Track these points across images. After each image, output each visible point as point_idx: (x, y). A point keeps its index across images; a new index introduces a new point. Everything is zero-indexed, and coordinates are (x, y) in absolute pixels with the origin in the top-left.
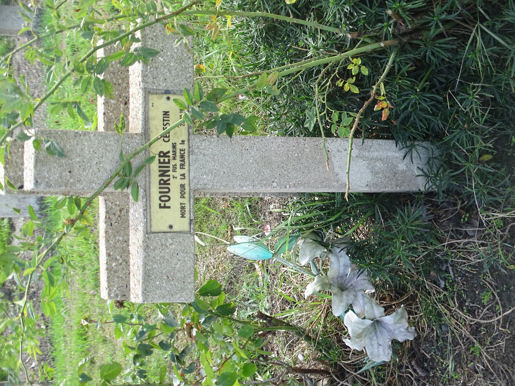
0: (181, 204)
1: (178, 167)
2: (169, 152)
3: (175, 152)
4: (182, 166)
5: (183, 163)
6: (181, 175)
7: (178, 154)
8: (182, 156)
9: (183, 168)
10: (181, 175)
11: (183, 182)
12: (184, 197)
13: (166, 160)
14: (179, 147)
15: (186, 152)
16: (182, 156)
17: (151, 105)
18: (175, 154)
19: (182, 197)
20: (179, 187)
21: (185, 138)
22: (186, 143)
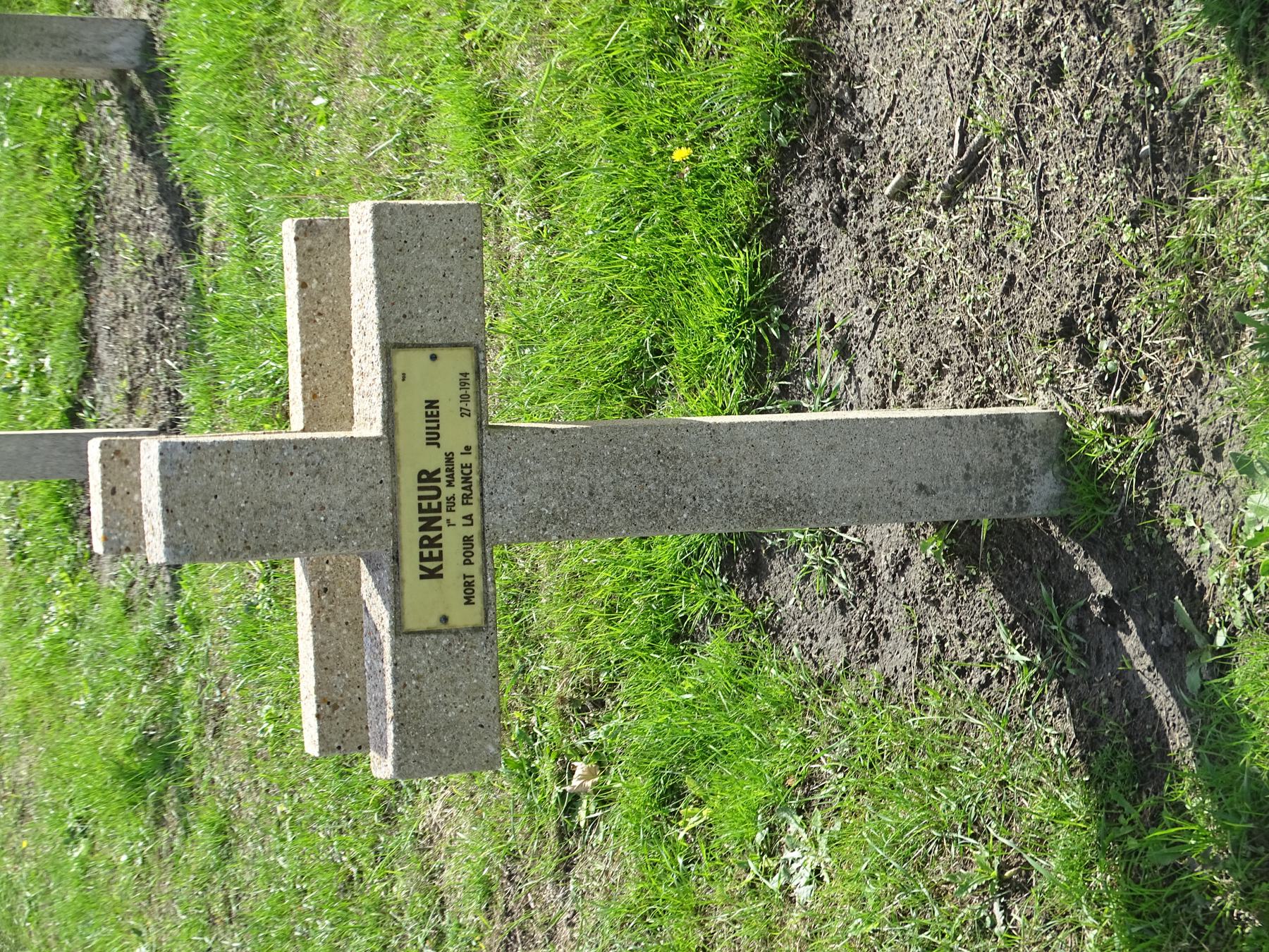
0: (465, 577)
1: (458, 500)
3: (452, 470)
4: (466, 499)
6: (464, 518)
7: (458, 477)
8: (466, 479)
9: (467, 503)
10: (464, 518)
12: (471, 563)
13: (434, 504)
14: (459, 460)
15: (474, 469)
18: (452, 476)
19: (468, 562)
21: (473, 443)
22: (474, 451)
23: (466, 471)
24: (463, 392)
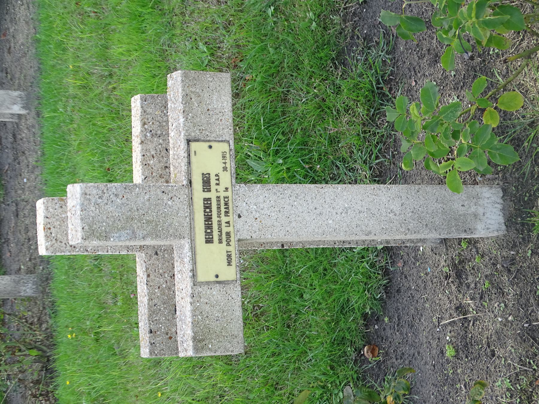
0: (227, 252)
4: (227, 213)
6: (226, 223)
8: (226, 204)
10: (226, 223)
12: (230, 245)
15: (230, 198)
17: (192, 154)
19: (228, 244)
21: (229, 186)
23: (226, 200)
24: (224, 161)
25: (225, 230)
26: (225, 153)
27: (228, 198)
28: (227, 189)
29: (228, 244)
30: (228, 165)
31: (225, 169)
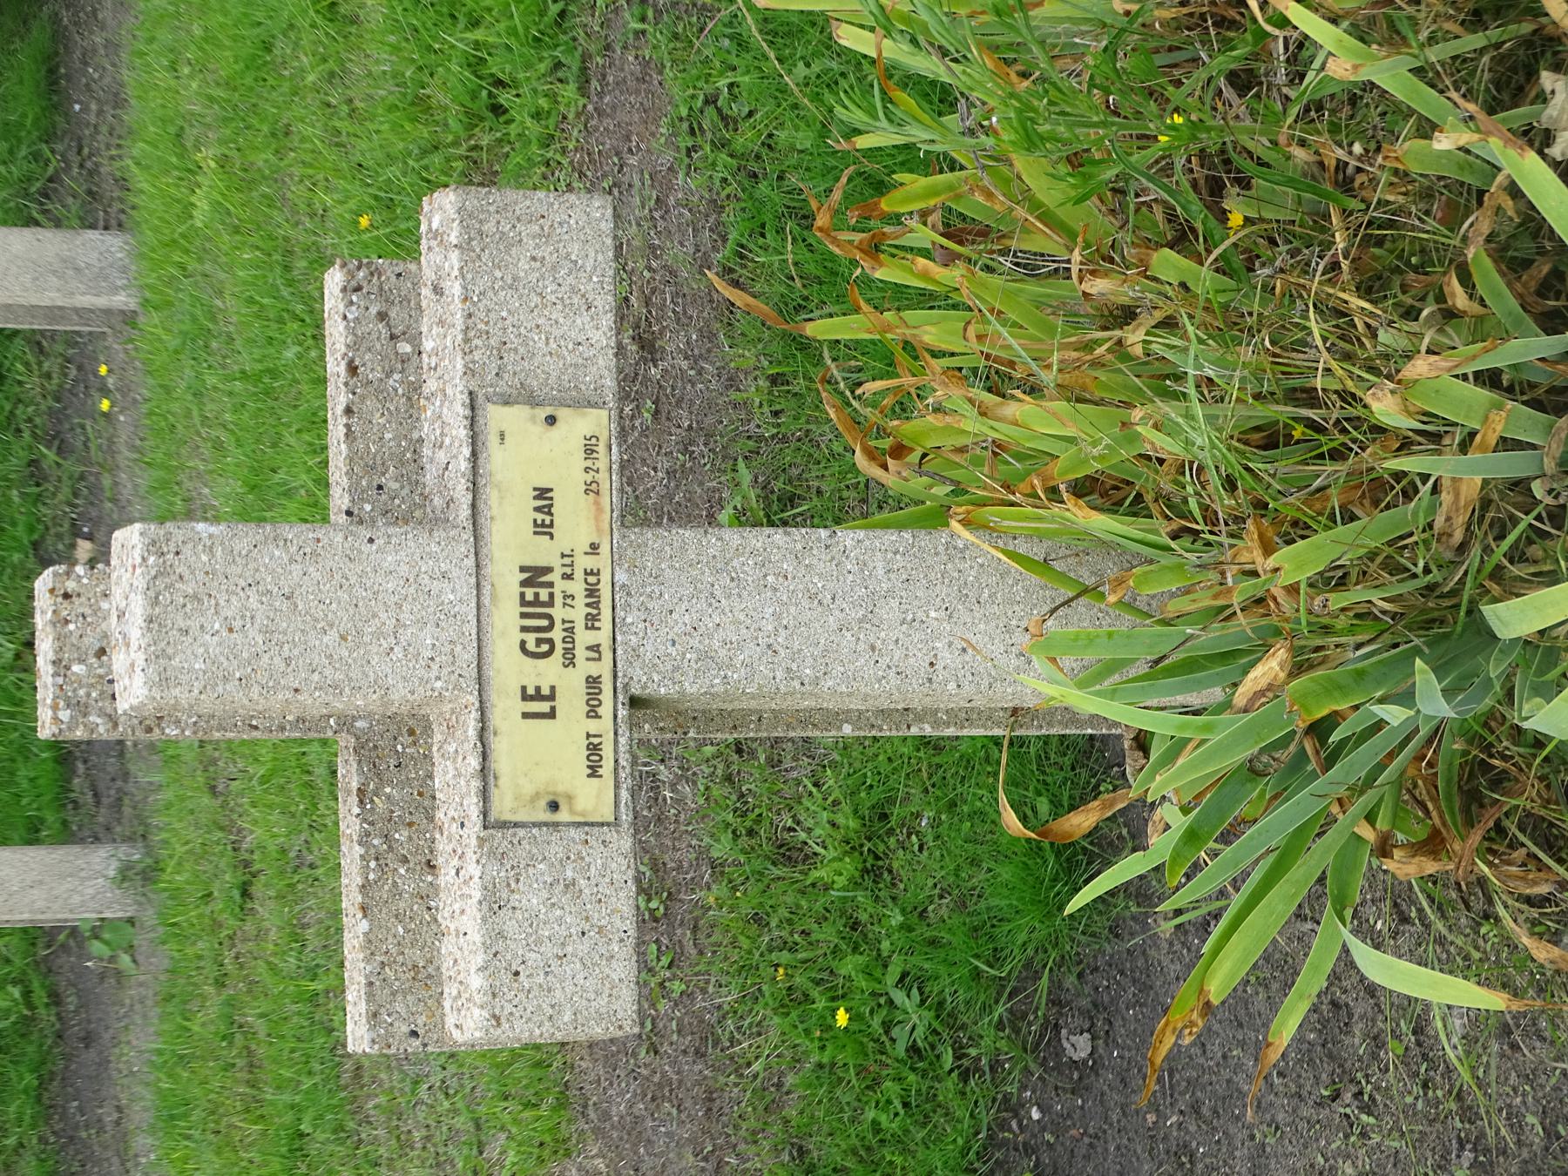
0: (588, 736)
2: (549, 570)
4: (592, 622)
5: (595, 612)
6: (588, 648)
8: (592, 592)
9: (593, 628)
10: (588, 648)
11: (593, 669)
12: (598, 717)
14: (583, 562)
15: (605, 577)
16: (592, 592)
17: (493, 440)
19: (593, 713)
20: (584, 684)
22: (605, 549)
24: (589, 463)
25: (584, 668)
26: (594, 441)
27: (598, 573)
28: (594, 548)
29: (593, 713)
30: (603, 477)
31: (591, 489)
